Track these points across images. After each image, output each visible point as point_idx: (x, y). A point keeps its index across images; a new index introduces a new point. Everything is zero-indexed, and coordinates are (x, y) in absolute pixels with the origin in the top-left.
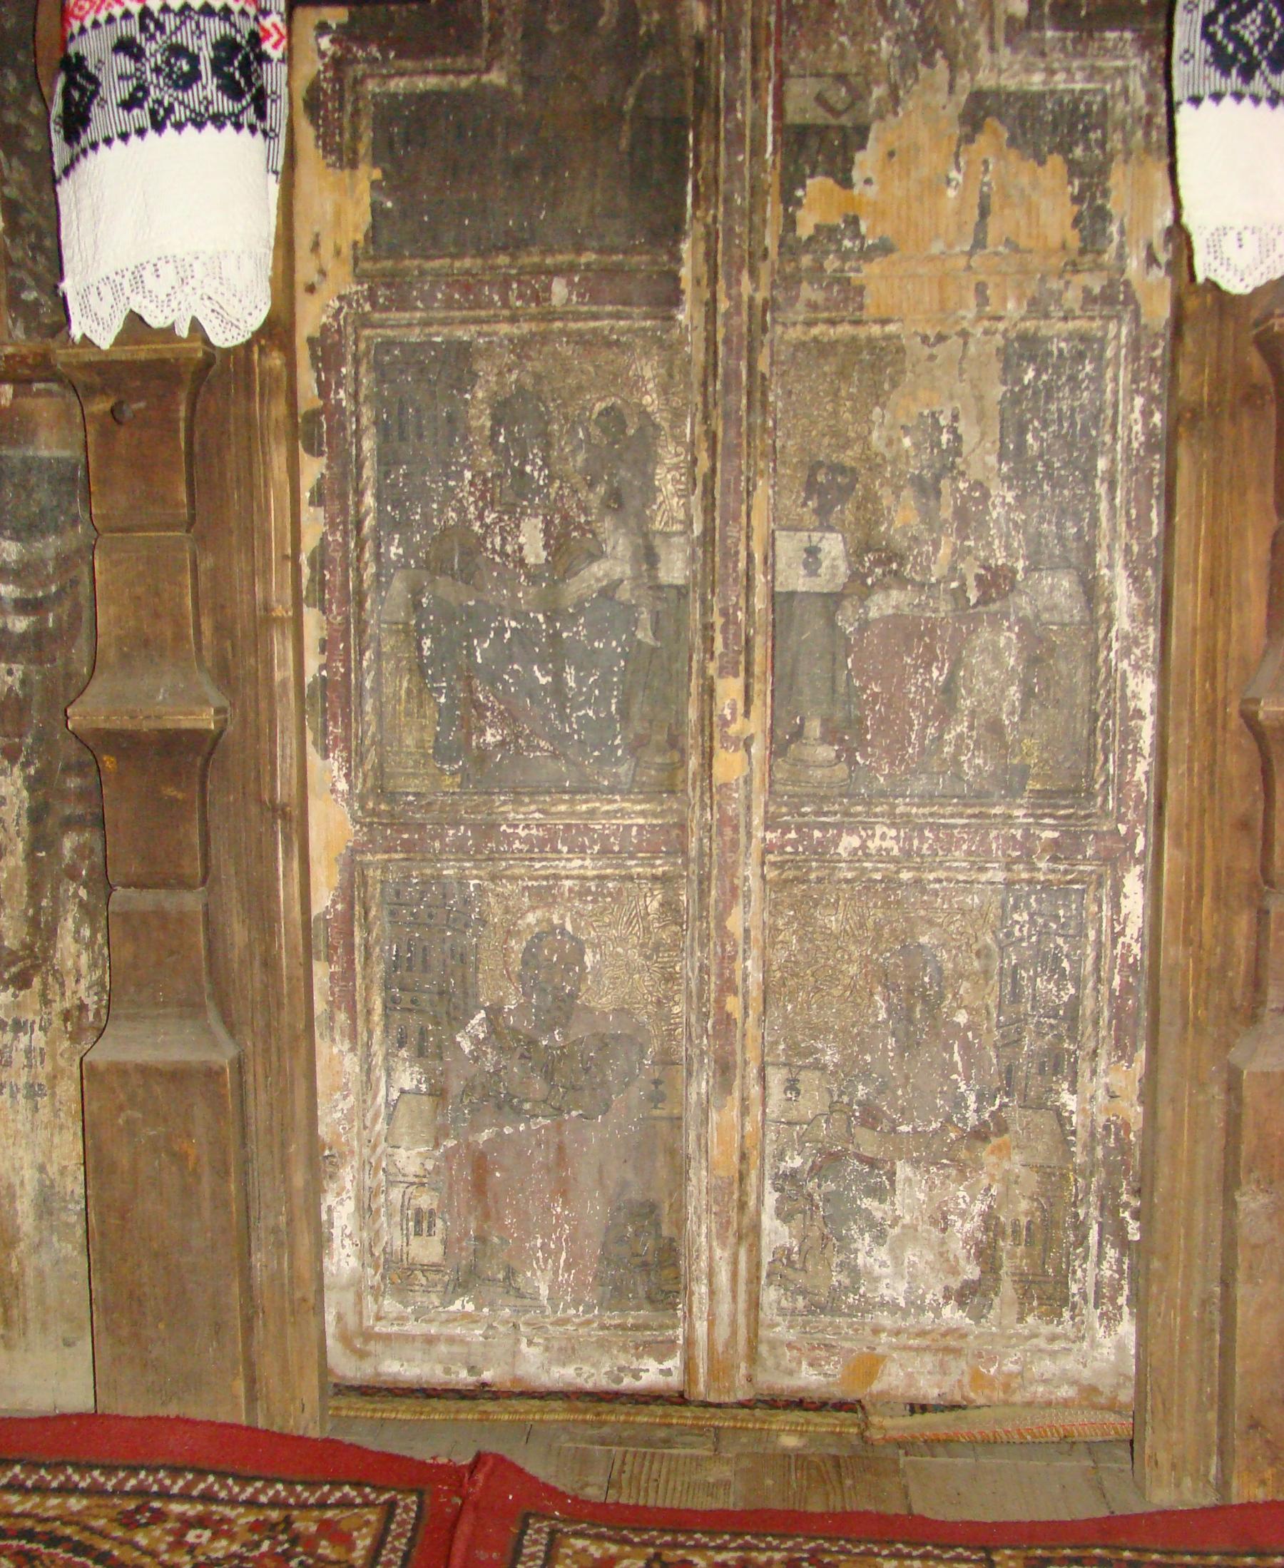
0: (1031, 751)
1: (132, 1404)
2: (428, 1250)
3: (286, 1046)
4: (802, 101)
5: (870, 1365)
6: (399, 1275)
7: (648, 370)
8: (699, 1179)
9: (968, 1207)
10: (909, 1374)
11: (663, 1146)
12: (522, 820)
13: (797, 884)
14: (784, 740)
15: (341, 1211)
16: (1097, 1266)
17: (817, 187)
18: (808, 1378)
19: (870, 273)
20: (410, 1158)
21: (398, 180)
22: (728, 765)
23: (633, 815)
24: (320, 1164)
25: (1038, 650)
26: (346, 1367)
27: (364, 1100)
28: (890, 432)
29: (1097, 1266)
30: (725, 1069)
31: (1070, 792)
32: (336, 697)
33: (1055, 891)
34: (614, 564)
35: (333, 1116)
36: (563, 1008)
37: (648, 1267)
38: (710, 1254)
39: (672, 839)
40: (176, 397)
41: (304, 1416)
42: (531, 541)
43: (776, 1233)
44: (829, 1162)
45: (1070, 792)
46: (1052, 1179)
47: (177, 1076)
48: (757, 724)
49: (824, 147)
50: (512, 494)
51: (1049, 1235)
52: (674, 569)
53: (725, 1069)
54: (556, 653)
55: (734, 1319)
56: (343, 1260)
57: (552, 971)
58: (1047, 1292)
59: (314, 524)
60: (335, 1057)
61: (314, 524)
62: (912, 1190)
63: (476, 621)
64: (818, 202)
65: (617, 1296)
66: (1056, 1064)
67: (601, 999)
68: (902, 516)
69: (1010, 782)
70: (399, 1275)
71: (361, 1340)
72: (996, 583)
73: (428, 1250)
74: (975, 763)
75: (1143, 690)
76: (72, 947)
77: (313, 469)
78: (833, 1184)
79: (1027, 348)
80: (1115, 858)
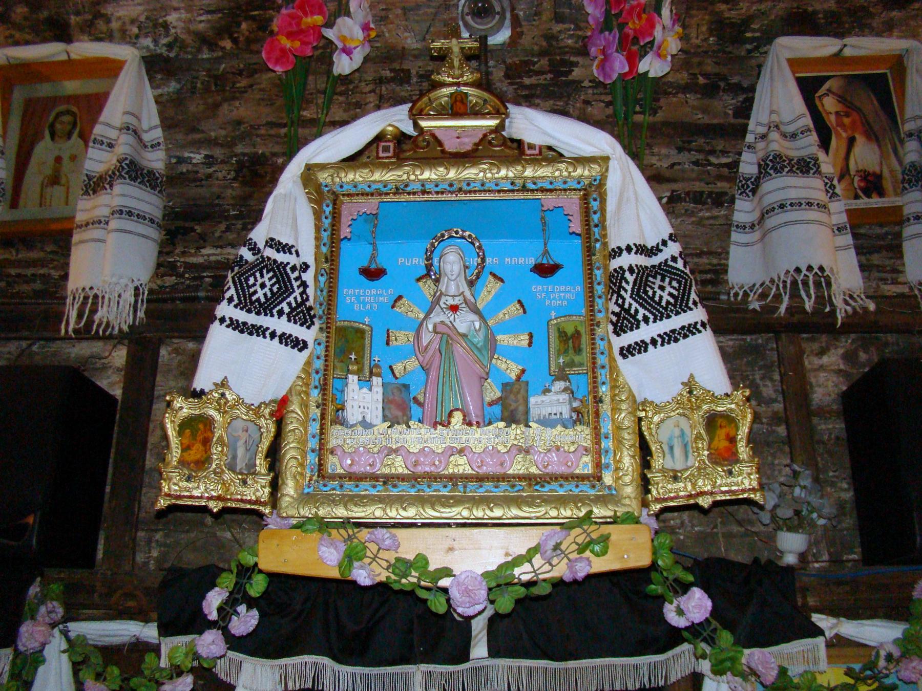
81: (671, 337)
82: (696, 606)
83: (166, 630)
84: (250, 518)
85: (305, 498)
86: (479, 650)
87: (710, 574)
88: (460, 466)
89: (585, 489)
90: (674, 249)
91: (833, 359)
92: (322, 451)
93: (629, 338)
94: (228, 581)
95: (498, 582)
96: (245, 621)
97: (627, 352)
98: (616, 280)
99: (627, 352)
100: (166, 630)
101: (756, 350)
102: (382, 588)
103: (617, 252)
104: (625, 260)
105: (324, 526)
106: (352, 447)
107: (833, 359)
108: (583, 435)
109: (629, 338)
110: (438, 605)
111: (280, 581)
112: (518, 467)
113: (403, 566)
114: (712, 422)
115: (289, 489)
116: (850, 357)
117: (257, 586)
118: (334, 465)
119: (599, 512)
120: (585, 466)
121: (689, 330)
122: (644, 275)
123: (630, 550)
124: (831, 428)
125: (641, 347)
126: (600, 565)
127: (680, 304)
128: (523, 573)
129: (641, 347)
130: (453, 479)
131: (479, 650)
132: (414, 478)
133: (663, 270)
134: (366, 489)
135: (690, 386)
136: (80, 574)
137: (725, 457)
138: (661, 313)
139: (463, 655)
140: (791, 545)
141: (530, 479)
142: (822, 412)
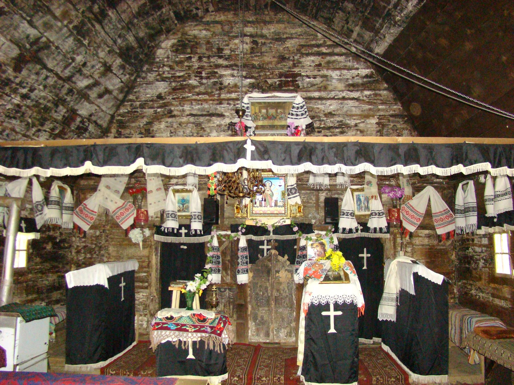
0: (289, 305)
1: (238, 342)
2: (255, 334)
3: (247, 322)
4: (276, 269)
5: (280, 340)
6: (253, 335)
7: (268, 284)
8: (270, 329)
9: (286, 331)
10: (283, 341)
11: (268, 328)
12: (261, 309)
13: (276, 312)
14: (275, 304)
15: (250, 331)
16: (293, 334)
17: (277, 274)
18: (277, 341)
19: (280, 279)
20: (254, 328)
21: (254, 274)
22: (272, 306)
23: (266, 308)
24: (249, 328)
25: (289, 299)
26: (250, 341)
27: (251, 325)
28: (281, 287)
29: (293, 334)
30: (272, 323)
31: (291, 307)
32: (251, 301)
33: (290, 313)
34: (266, 294)
35: (249, 326)
36: (263, 320)
37: (267, 335)
38: (271, 334)
39: (269, 310)
40: (242, 287)
41: (247, 343)
42: (261, 293)
43: (275, 333)
44: (278, 328)
45: (291, 307)
46: (291, 329)
47: (242, 323)
48: (274, 304)
49: (278, 272)
50: (260, 291)
51: (291, 333)
52: (269, 295)
53: (272, 323)
54: (263, 299)
55: (273, 338)
56: (250, 334)
57: (262, 317)
58: (290, 336)
59: (249, 292)
60: (250, 322)
61: (249, 292)
62: (283, 330)
63: (258, 298)
64: (277, 275)
65: (266, 336)
66: (291, 323)
67: (265, 319)
68: (282, 292)
69: (288, 307)
70: (253, 335)
71: (251, 339)
72: (287, 296)
73: (255, 334)
74: (286, 306)
75: (295, 302)
76: (235, 316)
77: (249, 289)
78: (278, 330)
79: (288, 283)
80: (294, 311)
81: (294, 197)
82: (296, 229)
83: (232, 232)
84: (243, 218)
85: (251, 216)
86: (271, 234)
87: (298, 225)
88: (269, 212)
89: (283, 215)
90: (295, 185)
91: (324, 194)
92: (252, 211)
93: (289, 197)
94: (242, 226)
95: (273, 226)
96: (244, 230)
97: (289, 198)
98: (288, 189)
99: (289, 198)
100: (232, 232)
101: (312, 193)
102: (260, 226)
103: (288, 186)
104: (289, 187)
105: (253, 219)
106: (256, 210)
107: (324, 194)
108: (283, 208)
109: (289, 197)
110: (266, 228)
111: (247, 226)
112: (276, 212)
113: (262, 224)
114: (299, 207)
115: (249, 215)
116: (327, 194)
117: (245, 226)
118: (254, 212)
119: (285, 218)
120: (284, 212)
121: (296, 196)
122: (291, 189)
123: (288, 222)
124: (322, 205)
125: (291, 198)
126: (284, 224)
127: (295, 193)
128: (276, 225)
129: (291, 198)
130: (268, 214)
131: (271, 234)
132: (263, 214)
133: (294, 188)
134: (258, 215)
135: (296, 203)
136: (217, 225)
137: (300, 212)
138: (293, 194)
139: (269, 235)
140: (313, 221)
141: (277, 214)
142: (321, 202)
